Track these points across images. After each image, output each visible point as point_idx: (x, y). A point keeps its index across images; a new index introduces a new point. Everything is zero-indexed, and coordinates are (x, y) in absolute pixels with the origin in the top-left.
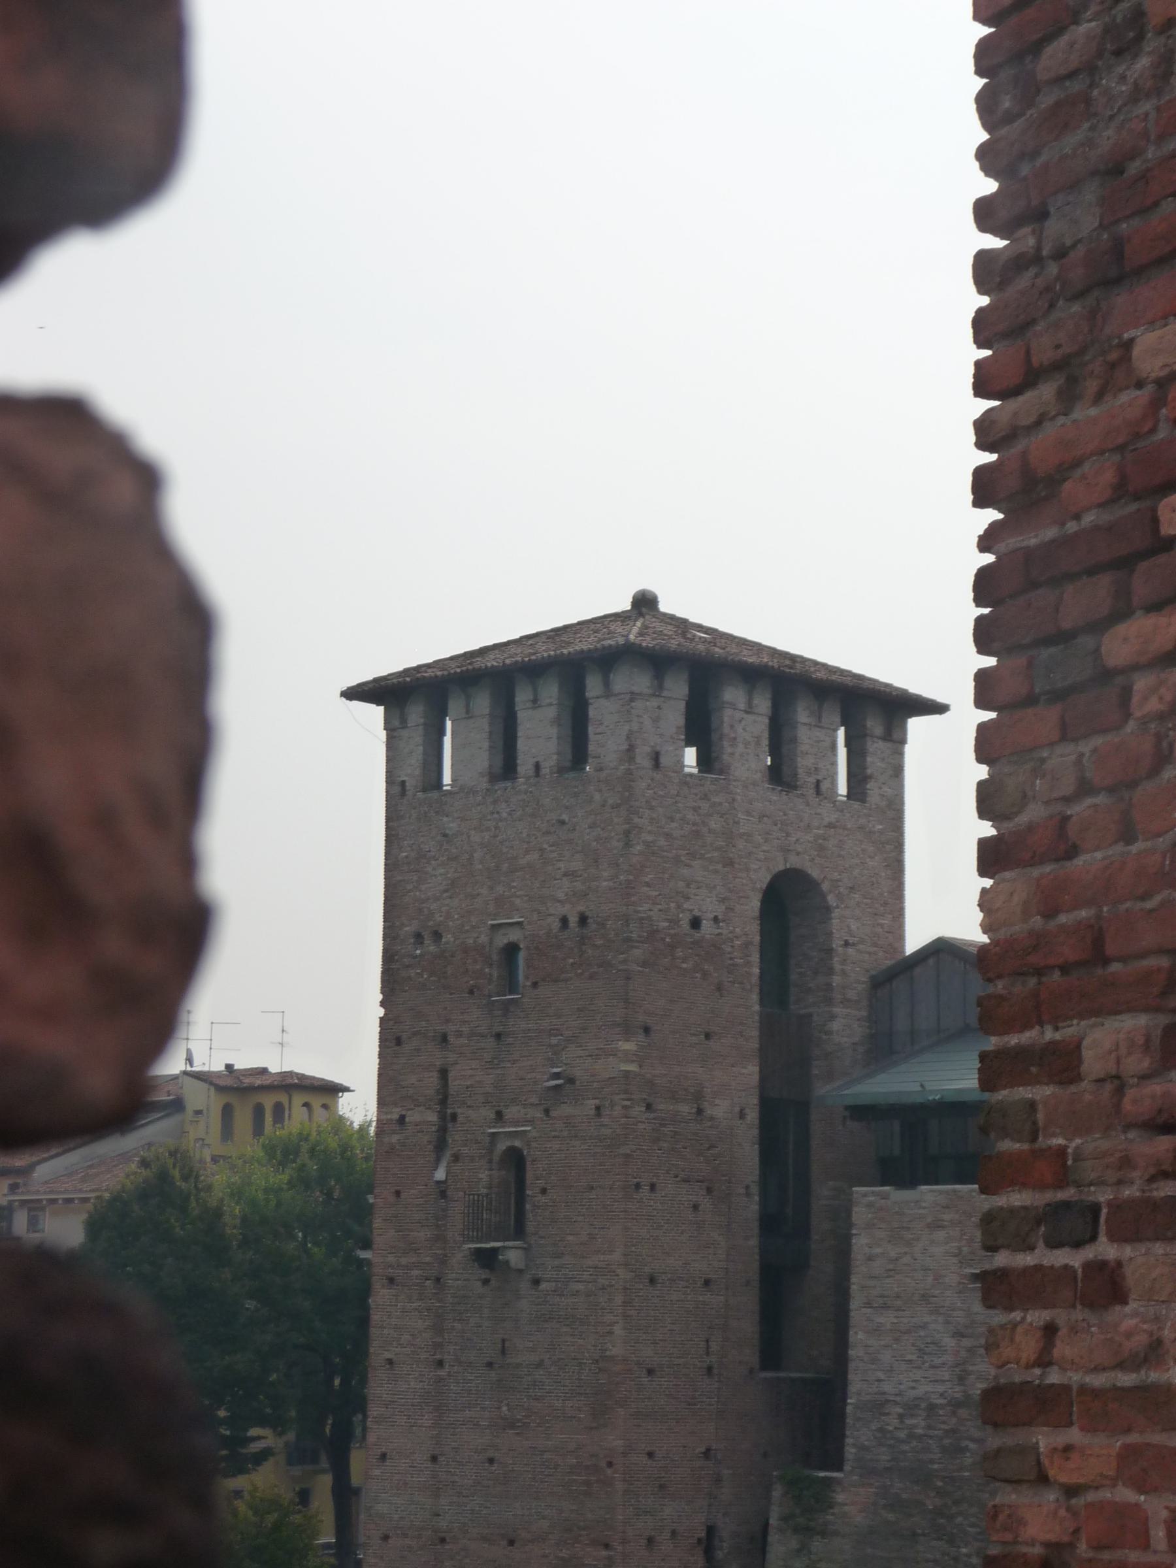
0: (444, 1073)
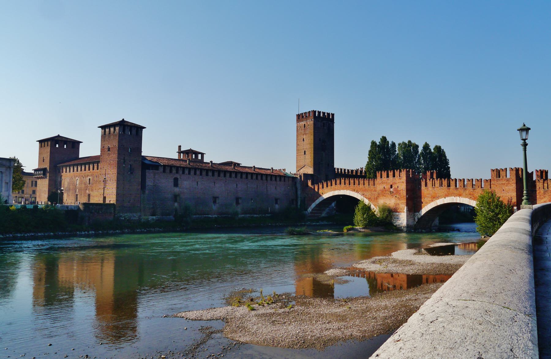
0: (124, 158)
